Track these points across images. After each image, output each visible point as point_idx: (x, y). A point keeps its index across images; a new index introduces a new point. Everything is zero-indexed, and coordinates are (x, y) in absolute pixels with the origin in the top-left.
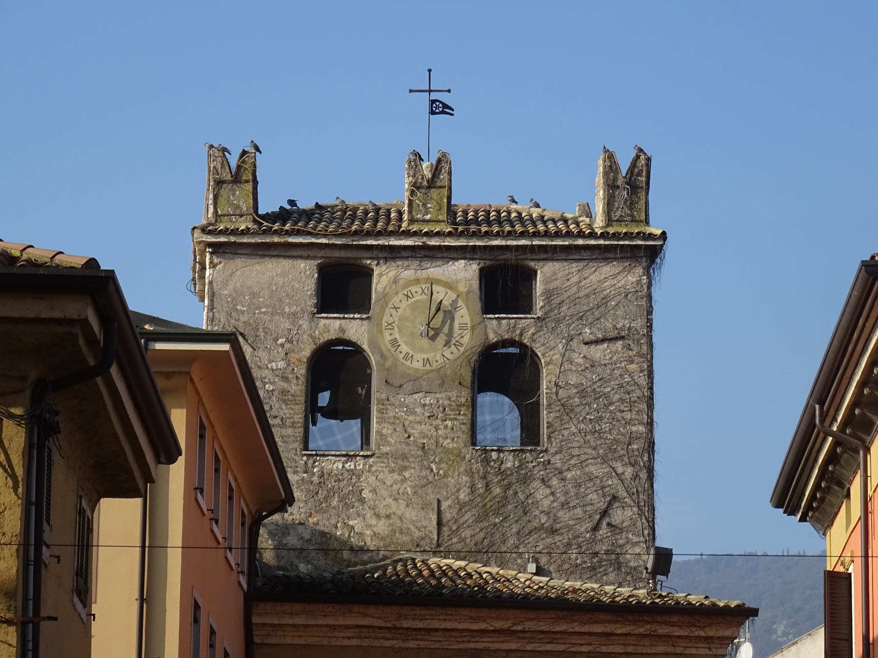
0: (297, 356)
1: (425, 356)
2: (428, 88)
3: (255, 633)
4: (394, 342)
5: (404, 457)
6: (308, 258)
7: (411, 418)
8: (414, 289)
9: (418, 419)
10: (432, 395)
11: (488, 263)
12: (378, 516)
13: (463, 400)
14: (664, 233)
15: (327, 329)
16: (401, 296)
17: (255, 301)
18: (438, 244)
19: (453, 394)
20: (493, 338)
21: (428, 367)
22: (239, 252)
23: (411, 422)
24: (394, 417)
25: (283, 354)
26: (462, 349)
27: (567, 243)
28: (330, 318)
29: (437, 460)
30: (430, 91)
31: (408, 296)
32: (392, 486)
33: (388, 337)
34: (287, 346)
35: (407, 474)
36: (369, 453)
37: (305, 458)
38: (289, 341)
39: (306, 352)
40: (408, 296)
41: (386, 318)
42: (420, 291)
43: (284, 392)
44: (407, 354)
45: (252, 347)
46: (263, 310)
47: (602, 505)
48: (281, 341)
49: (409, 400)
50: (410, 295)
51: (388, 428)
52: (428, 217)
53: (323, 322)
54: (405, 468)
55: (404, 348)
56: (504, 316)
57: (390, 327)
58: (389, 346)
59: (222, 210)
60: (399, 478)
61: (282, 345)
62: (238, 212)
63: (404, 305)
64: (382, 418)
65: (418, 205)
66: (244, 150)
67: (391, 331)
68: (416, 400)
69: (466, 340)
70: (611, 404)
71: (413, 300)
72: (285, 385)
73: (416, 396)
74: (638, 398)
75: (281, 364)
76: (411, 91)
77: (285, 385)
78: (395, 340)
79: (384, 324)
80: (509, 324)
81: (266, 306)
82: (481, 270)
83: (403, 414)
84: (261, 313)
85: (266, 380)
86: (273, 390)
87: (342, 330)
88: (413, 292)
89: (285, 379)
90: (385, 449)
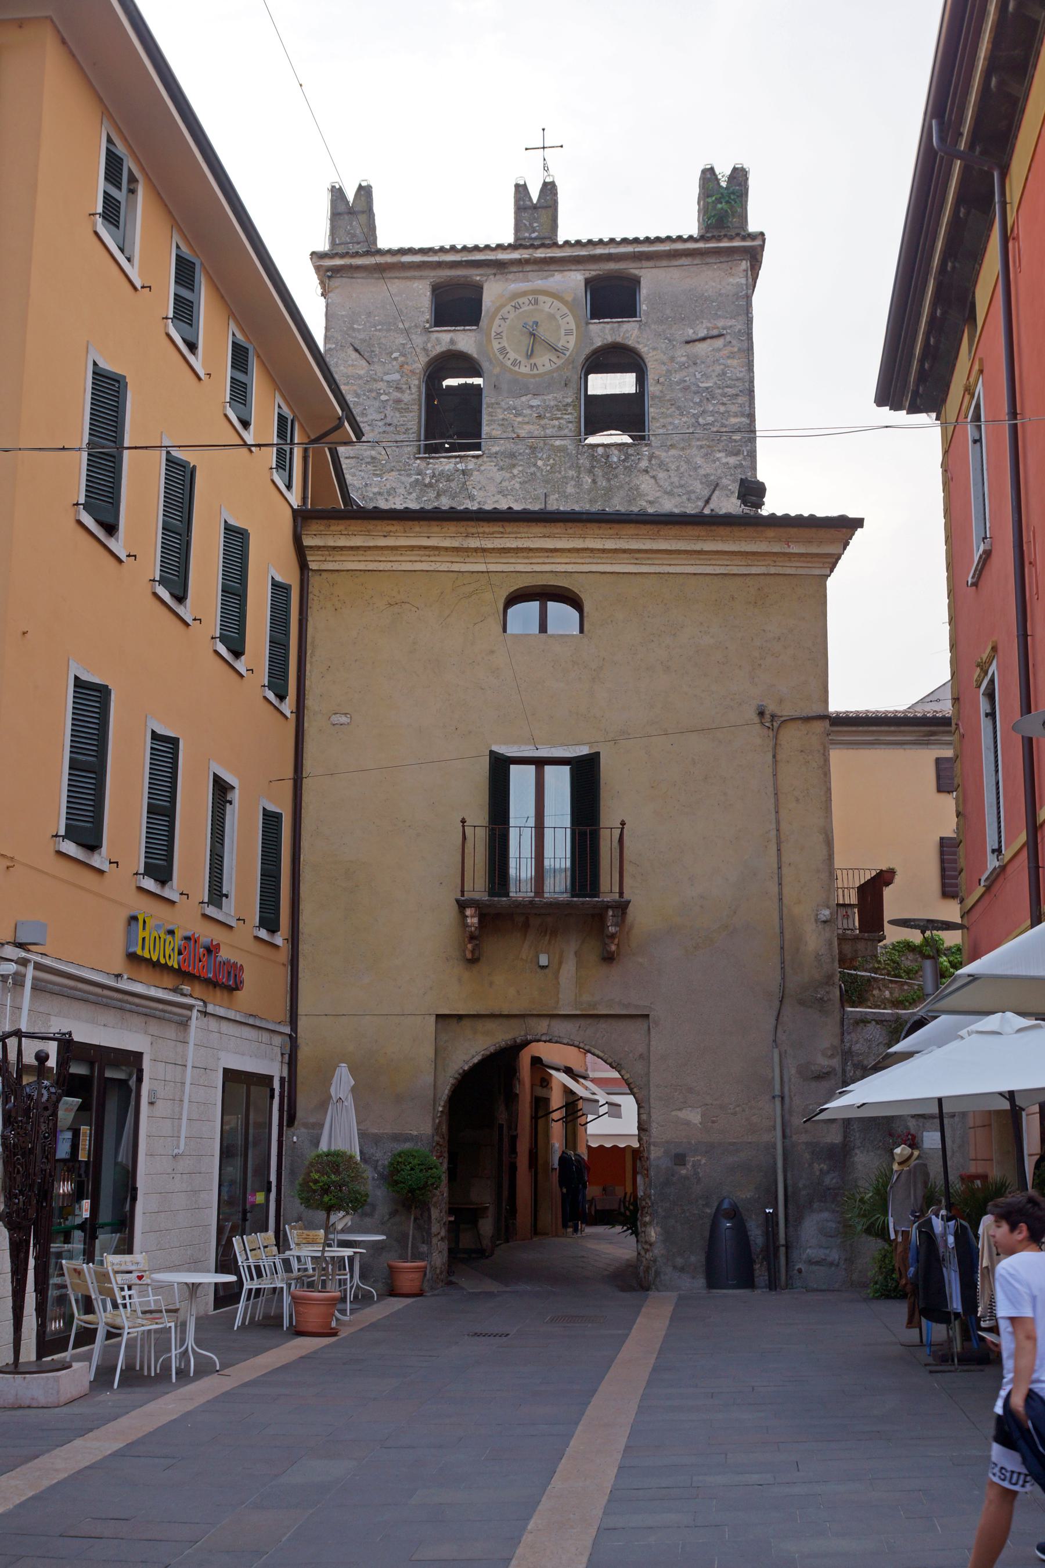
0: (410, 368)
3: (309, 558)
4: (503, 350)
6: (421, 278)
7: (520, 419)
8: (521, 300)
9: (526, 419)
10: (540, 397)
11: (594, 273)
13: (569, 400)
15: (437, 339)
16: (509, 307)
18: (543, 255)
19: (559, 396)
20: (598, 343)
21: (535, 372)
22: (355, 275)
23: (519, 423)
24: (503, 419)
25: (397, 367)
27: (668, 248)
28: (441, 331)
29: (544, 456)
30: (544, 148)
31: (515, 307)
32: (500, 483)
33: (496, 345)
34: (401, 359)
35: (515, 472)
36: (480, 453)
37: (418, 461)
38: (404, 355)
39: (419, 363)
40: (515, 307)
41: (495, 328)
43: (398, 401)
44: (516, 360)
45: (368, 362)
46: (378, 328)
47: (706, 493)
49: (518, 402)
50: (517, 306)
51: (497, 430)
52: (534, 235)
53: (436, 335)
54: (514, 466)
55: (512, 355)
56: (609, 320)
57: (499, 336)
58: (498, 354)
59: (340, 239)
61: (396, 359)
62: (355, 240)
63: (512, 315)
64: (492, 420)
65: (525, 225)
66: (360, 185)
67: (499, 340)
68: (523, 402)
70: (713, 398)
71: (521, 310)
72: (397, 395)
73: (524, 399)
74: (741, 391)
75: (396, 376)
76: (526, 149)
77: (397, 395)
78: (504, 348)
79: (493, 334)
80: (612, 329)
82: (588, 282)
83: (511, 416)
85: (382, 391)
86: (387, 400)
87: (452, 342)
88: (520, 303)
89: (398, 389)
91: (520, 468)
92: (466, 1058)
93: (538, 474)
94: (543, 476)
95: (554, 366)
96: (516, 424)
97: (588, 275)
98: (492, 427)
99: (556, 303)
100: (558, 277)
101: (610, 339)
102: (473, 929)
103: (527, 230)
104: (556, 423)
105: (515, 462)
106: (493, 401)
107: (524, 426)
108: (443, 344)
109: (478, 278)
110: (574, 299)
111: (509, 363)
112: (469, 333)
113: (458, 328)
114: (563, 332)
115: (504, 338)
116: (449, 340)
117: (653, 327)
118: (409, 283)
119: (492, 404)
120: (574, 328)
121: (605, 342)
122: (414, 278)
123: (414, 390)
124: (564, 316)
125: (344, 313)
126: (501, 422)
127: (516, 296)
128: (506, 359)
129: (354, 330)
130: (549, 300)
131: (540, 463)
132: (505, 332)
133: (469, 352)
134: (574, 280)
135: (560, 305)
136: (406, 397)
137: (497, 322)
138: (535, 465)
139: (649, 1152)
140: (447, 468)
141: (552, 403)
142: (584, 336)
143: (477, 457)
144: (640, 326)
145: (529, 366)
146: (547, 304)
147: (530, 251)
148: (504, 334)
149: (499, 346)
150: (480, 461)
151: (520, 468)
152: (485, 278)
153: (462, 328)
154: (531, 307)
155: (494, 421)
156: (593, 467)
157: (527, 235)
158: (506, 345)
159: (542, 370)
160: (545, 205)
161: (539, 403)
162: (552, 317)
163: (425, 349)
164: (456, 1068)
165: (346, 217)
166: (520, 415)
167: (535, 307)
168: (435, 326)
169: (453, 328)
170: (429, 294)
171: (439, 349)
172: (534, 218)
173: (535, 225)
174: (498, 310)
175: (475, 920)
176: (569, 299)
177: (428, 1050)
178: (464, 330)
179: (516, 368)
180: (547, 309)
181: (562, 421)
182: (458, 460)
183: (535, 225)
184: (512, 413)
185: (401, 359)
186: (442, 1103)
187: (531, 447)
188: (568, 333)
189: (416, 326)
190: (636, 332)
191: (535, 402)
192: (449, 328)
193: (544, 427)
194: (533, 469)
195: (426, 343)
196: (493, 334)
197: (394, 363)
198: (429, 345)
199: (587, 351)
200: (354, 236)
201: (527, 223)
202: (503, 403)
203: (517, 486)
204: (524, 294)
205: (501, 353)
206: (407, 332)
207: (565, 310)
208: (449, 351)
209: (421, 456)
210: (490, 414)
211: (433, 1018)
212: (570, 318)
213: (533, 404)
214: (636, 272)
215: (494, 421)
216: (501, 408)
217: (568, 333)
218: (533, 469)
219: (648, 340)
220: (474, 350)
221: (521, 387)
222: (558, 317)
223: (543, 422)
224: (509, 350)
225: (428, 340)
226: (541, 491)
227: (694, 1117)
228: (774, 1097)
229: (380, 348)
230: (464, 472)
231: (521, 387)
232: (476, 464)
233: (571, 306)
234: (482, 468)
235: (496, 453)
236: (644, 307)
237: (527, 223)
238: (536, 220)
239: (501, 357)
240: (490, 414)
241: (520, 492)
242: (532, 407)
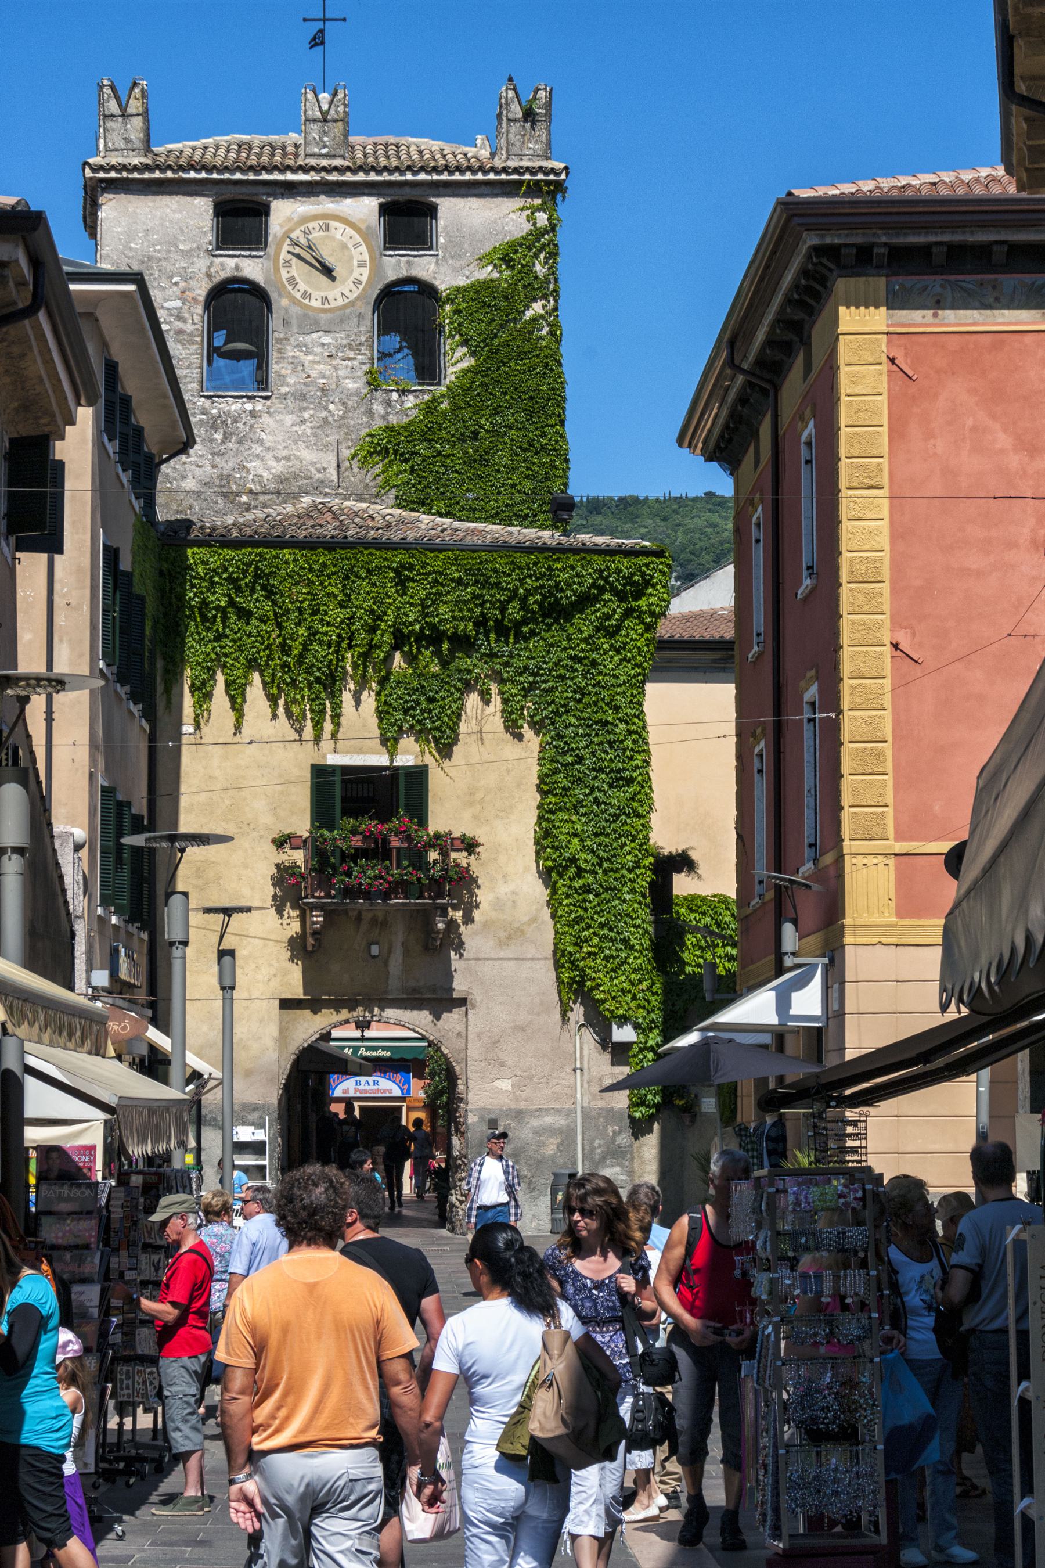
0: (191, 295)
1: (324, 294)
4: (292, 280)
5: (303, 397)
7: (310, 358)
8: (311, 225)
9: (317, 359)
10: (332, 335)
12: (277, 459)
14: (566, 168)
15: (222, 265)
17: (150, 238)
20: (392, 276)
21: (326, 306)
23: (310, 362)
24: (293, 357)
25: (178, 293)
26: (361, 287)
30: (324, 20)
31: (305, 232)
34: (182, 284)
35: (306, 415)
36: (269, 394)
37: (203, 399)
39: (201, 291)
42: (318, 228)
43: (180, 332)
44: (306, 292)
46: (159, 247)
48: (175, 279)
52: (325, 151)
54: (305, 409)
55: (302, 286)
58: (287, 284)
60: (298, 420)
61: (176, 284)
62: (130, 146)
69: (364, 279)
72: (179, 325)
73: (314, 335)
75: (178, 303)
77: (179, 325)
79: (281, 261)
80: (408, 262)
81: (161, 244)
82: (381, 206)
84: (155, 251)
87: (237, 268)
88: (311, 228)
89: (180, 318)
90: (284, 390)
91: (311, 412)
92: (305, 1036)
93: (330, 419)
94: (335, 421)
95: (346, 301)
96: (306, 364)
97: (382, 200)
98: (281, 365)
99: (348, 229)
100: (349, 201)
101: (404, 273)
104: (349, 363)
105: (306, 405)
106: (282, 336)
107: (316, 366)
108: (228, 270)
110: (368, 228)
111: (298, 295)
112: (256, 260)
114: (355, 263)
115: (294, 267)
116: (233, 266)
117: (450, 262)
119: (281, 340)
120: (368, 259)
121: (401, 276)
123: (197, 319)
124: (357, 245)
125: (119, 229)
126: (290, 360)
127: (305, 219)
129: (131, 249)
130: (341, 226)
131: (331, 407)
134: (366, 208)
135: (353, 233)
136: (189, 327)
138: (326, 409)
139: (466, 1117)
140: (233, 408)
141: (345, 342)
142: (377, 269)
143: (267, 398)
144: (437, 260)
145: (320, 300)
146: (340, 232)
147: (323, 174)
149: (289, 275)
150: (268, 403)
151: (311, 412)
153: (247, 253)
154: (322, 233)
155: (284, 358)
156: (388, 414)
157: (316, 150)
158: (296, 275)
159: (333, 304)
160: (336, 117)
161: (330, 341)
162: (344, 246)
163: (209, 276)
164: (297, 1045)
165: (120, 119)
166: (310, 353)
167: (326, 233)
168: (218, 248)
170: (211, 211)
171: (223, 275)
172: (324, 131)
173: (326, 139)
175: (321, 919)
176: (363, 226)
177: (272, 1030)
179: (307, 301)
180: (338, 236)
181: (356, 363)
182: (245, 400)
183: (326, 139)
184: (302, 351)
185: (182, 284)
186: (285, 1077)
187: (322, 390)
188: (362, 264)
189: (198, 248)
190: (432, 267)
191: (327, 339)
193: (336, 368)
194: (324, 414)
195: (209, 267)
196: (281, 261)
197: (175, 289)
199: (380, 286)
200: (127, 140)
201: (317, 137)
202: (292, 339)
203: (309, 432)
204: (315, 217)
205: (290, 284)
206: (187, 254)
207: (358, 238)
209: (206, 394)
210: (279, 351)
211: (277, 1003)
212: (363, 248)
213: (325, 342)
214: (433, 200)
215: (284, 358)
216: (290, 344)
217: (362, 264)
218: (324, 414)
219: (446, 276)
221: (311, 323)
222: (350, 246)
223: (335, 362)
224: (298, 280)
226: (332, 438)
227: (505, 1085)
228: (575, 1070)
229: (160, 271)
230: (253, 414)
231: (311, 323)
232: (264, 405)
233: (366, 235)
234: (272, 410)
235: (286, 394)
236: (442, 240)
237: (317, 137)
238: (325, 133)
239: (290, 288)
240: (279, 351)
241: (311, 438)
242: (323, 345)
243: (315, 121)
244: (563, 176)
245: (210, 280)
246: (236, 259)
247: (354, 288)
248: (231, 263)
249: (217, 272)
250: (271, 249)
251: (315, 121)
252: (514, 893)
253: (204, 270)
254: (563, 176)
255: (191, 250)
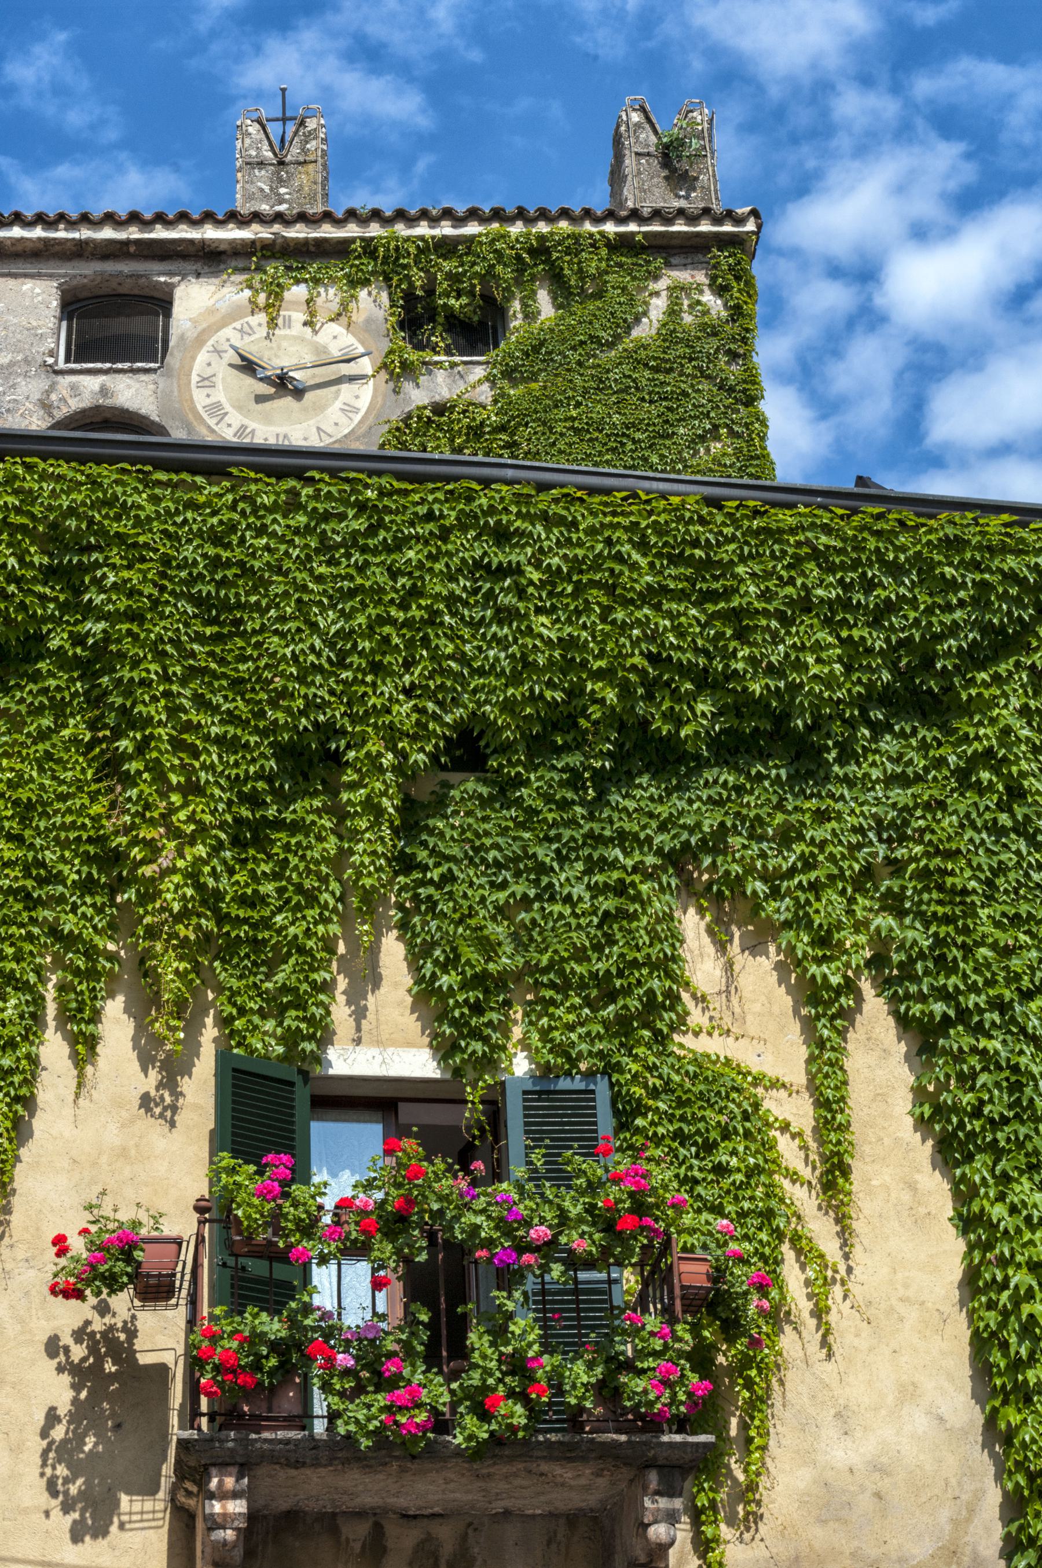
2: (280, 115)
6: (38, 276)
14: (755, 213)
15: (73, 387)
26: (357, 418)
31: (241, 331)
50: (246, 328)
65: (262, 190)
79: (195, 378)
87: (104, 391)
102: (230, 1534)
103: (266, 197)
109: (162, 279)
112: (144, 377)
113: (120, 366)
115: (220, 386)
116: (96, 388)
118: (11, 283)
122: (26, 276)
128: (222, 425)
132: (220, 376)
133: (143, 411)
137: (202, 357)
147: (277, 228)
148: (218, 380)
152: (177, 279)
153: (127, 365)
158: (223, 400)
169: (108, 365)
170: (55, 303)
171: (75, 404)
173: (282, 190)
174: (200, 341)
178: (132, 371)
189: (26, 361)
192: (99, 365)
195: (48, 393)
198: (54, 397)
201: (267, 189)
208: (97, 409)
220: (153, 407)
224: (228, 407)
225: (52, 387)
237: (267, 189)
238: (281, 181)
239: (212, 422)
243: (261, 164)
244: (750, 226)
245: (51, 415)
246: (102, 379)
247: (343, 420)
248: (91, 384)
249: (63, 400)
250: (174, 359)
251: (261, 164)
252: (879, 1468)
253: (36, 396)
254: (750, 226)
255: (12, 364)
